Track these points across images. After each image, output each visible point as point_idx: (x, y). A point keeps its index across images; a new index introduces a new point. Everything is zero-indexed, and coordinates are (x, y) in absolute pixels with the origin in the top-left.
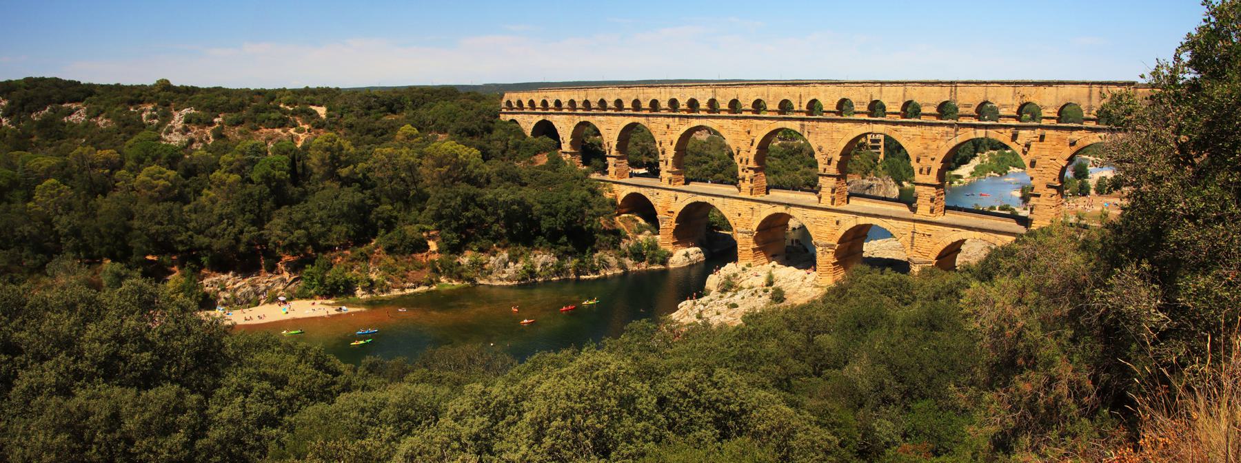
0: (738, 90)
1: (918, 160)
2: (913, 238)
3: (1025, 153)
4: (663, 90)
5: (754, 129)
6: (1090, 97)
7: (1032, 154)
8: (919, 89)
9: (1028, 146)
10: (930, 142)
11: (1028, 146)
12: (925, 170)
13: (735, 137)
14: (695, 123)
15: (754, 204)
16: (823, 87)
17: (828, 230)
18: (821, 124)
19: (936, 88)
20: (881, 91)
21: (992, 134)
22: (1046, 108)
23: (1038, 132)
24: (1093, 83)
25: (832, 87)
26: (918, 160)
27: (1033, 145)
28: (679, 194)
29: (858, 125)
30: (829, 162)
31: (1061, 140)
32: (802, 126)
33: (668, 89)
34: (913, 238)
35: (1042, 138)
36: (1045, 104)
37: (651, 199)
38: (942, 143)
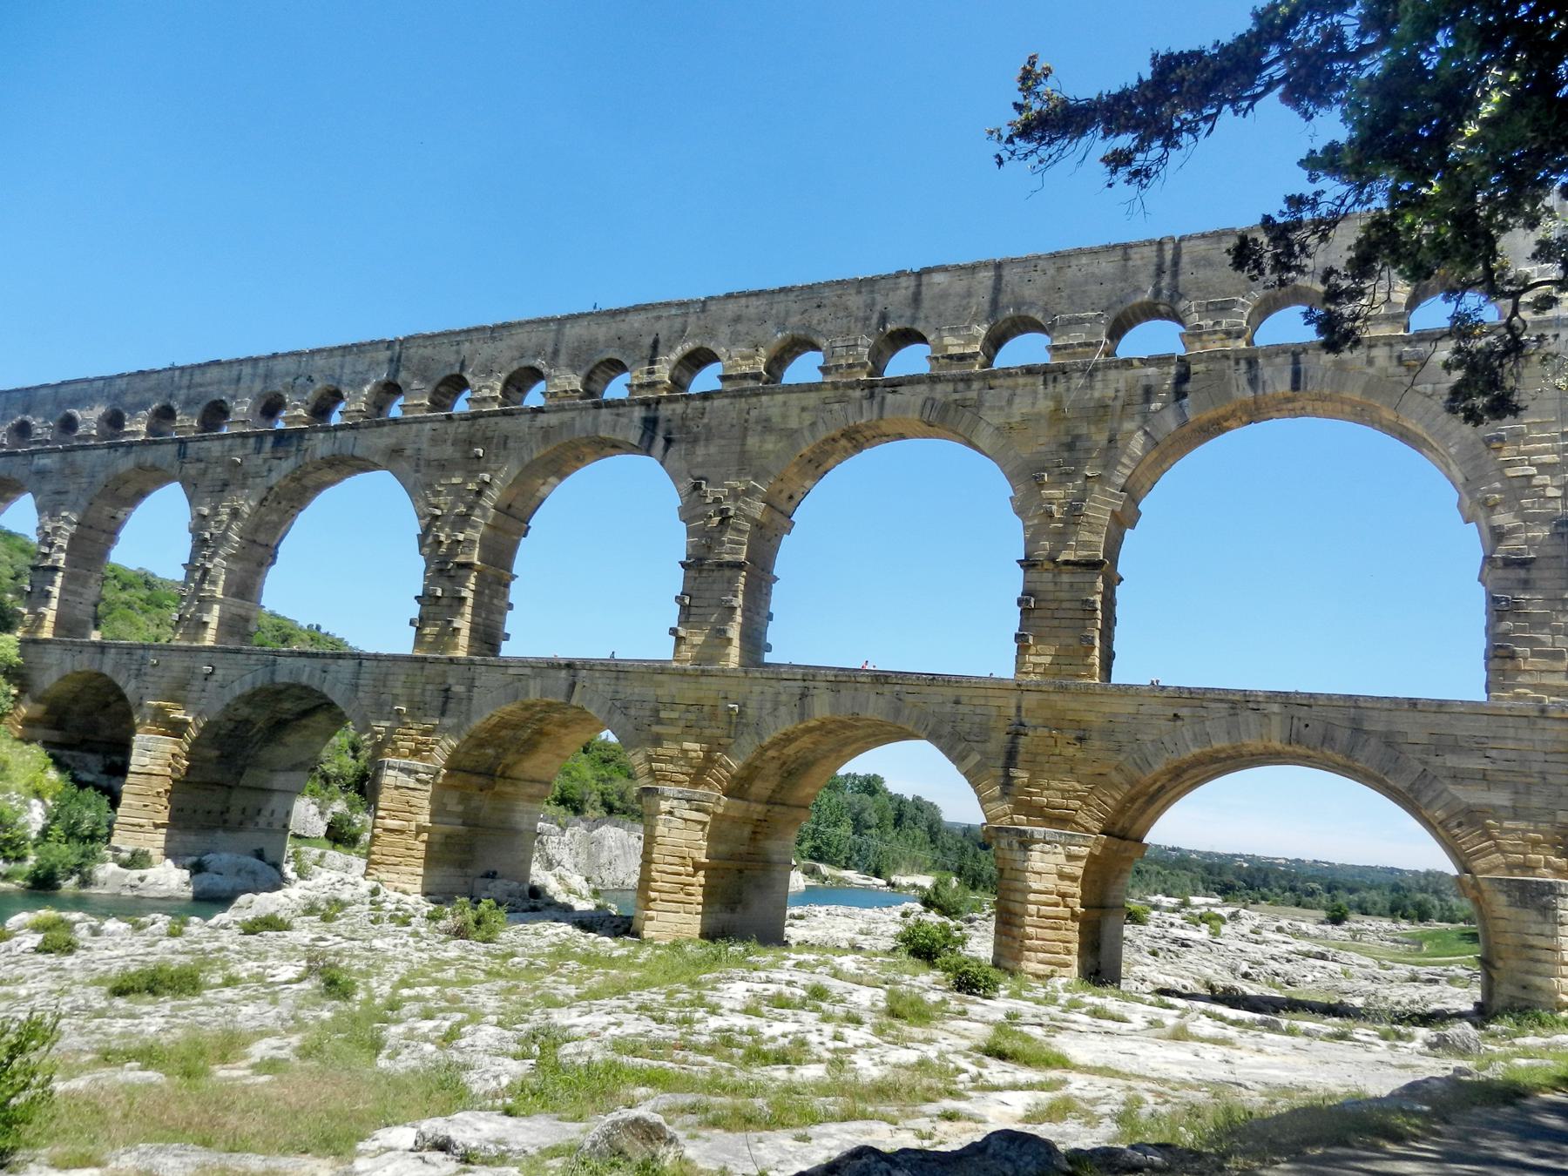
16: (732, 308)
20: (916, 299)
32: (650, 424)
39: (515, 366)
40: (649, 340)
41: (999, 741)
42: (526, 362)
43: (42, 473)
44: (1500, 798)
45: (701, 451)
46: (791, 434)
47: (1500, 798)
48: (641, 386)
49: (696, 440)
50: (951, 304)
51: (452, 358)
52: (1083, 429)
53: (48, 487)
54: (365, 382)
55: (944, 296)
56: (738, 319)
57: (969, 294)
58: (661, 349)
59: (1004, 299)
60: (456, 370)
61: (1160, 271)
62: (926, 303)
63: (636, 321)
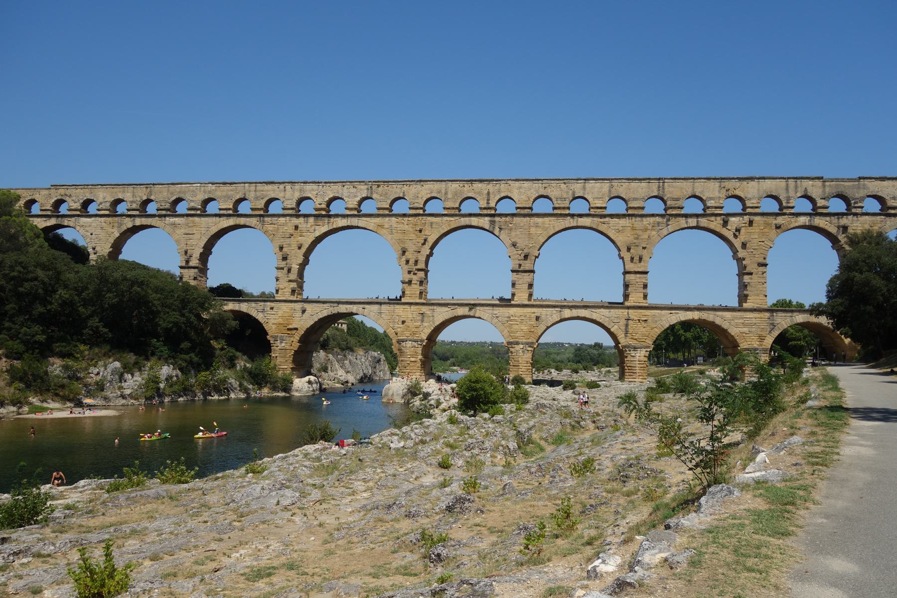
0: (405, 188)
1: (629, 249)
2: (627, 325)
3: (735, 236)
4: (288, 187)
5: (427, 227)
6: (787, 189)
7: (742, 237)
8: (626, 185)
9: (738, 230)
10: (640, 233)
11: (738, 230)
12: (636, 259)
13: (401, 236)
14: (341, 222)
15: (424, 309)
16: (517, 184)
17: (525, 328)
18: (517, 220)
19: (644, 184)
20: (584, 188)
21: (703, 222)
22: (750, 199)
23: (746, 218)
24: (789, 178)
25: (526, 184)
26: (629, 249)
27: (743, 231)
28: (306, 306)
29: (561, 220)
30: (526, 257)
31: (767, 225)
32: (493, 223)
33: (297, 187)
34: (627, 325)
35: (751, 223)
36: (749, 196)
37: (260, 317)
38: (654, 233)
39: (429, 196)
40: (486, 192)
41: (623, 322)
42: (433, 195)
43: (174, 225)
44: (746, 330)
45: (513, 234)
46: (546, 229)
47: (746, 330)
48: (485, 208)
49: (511, 229)
50: (596, 190)
51: (398, 190)
52: (640, 233)
53: (180, 232)
54: (355, 196)
55: (593, 188)
56: (520, 188)
57: (601, 188)
58: (492, 196)
59: (613, 190)
60: (401, 195)
61: (659, 187)
62: (588, 190)
63: (480, 185)
